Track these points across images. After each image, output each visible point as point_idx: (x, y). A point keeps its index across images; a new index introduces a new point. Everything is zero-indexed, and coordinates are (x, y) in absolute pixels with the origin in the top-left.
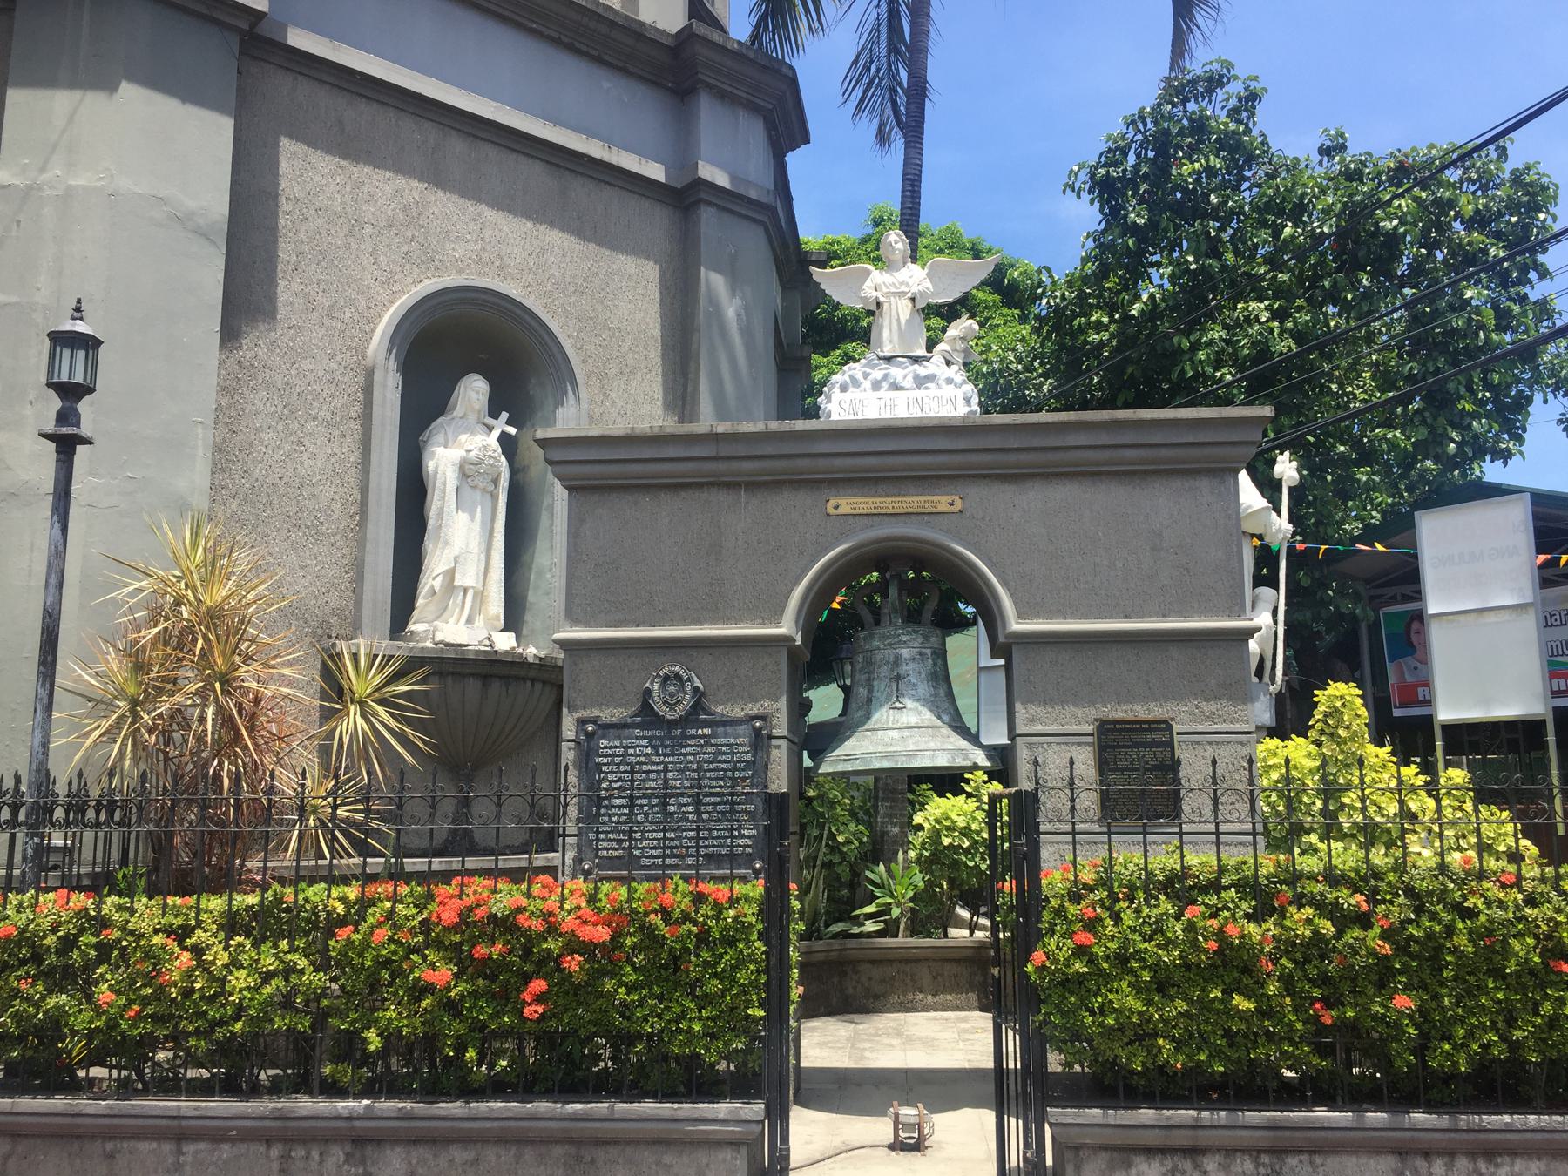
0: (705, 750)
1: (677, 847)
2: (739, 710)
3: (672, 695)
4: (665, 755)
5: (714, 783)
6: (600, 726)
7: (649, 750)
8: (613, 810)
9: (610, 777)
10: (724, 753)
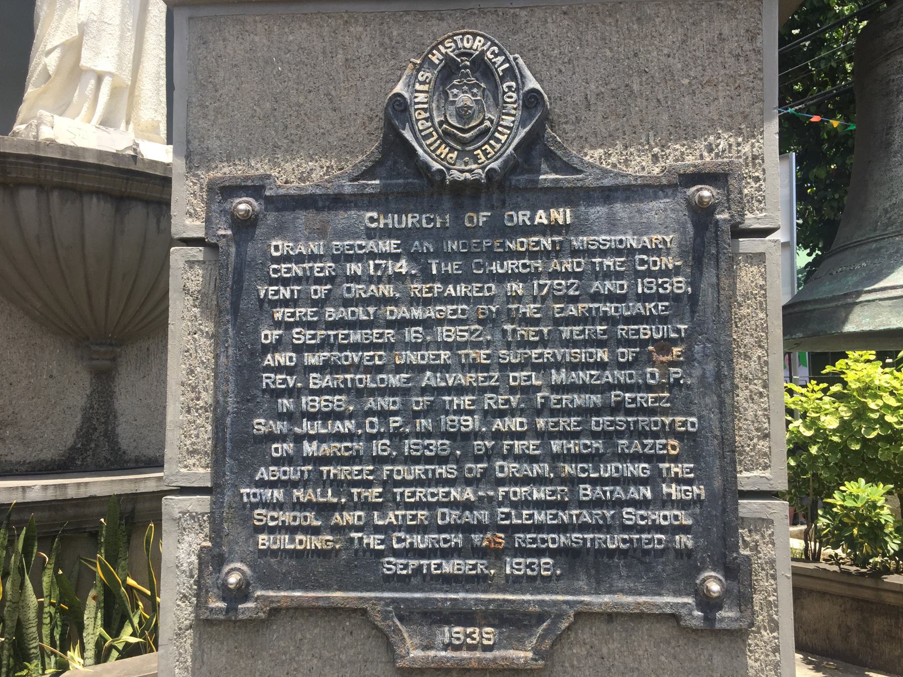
0: (554, 265)
1: (481, 528)
2: (646, 161)
3: (463, 114)
4: (446, 279)
5: (581, 354)
6: (270, 201)
7: (403, 266)
8: (306, 426)
9: (301, 336)
10: (608, 275)
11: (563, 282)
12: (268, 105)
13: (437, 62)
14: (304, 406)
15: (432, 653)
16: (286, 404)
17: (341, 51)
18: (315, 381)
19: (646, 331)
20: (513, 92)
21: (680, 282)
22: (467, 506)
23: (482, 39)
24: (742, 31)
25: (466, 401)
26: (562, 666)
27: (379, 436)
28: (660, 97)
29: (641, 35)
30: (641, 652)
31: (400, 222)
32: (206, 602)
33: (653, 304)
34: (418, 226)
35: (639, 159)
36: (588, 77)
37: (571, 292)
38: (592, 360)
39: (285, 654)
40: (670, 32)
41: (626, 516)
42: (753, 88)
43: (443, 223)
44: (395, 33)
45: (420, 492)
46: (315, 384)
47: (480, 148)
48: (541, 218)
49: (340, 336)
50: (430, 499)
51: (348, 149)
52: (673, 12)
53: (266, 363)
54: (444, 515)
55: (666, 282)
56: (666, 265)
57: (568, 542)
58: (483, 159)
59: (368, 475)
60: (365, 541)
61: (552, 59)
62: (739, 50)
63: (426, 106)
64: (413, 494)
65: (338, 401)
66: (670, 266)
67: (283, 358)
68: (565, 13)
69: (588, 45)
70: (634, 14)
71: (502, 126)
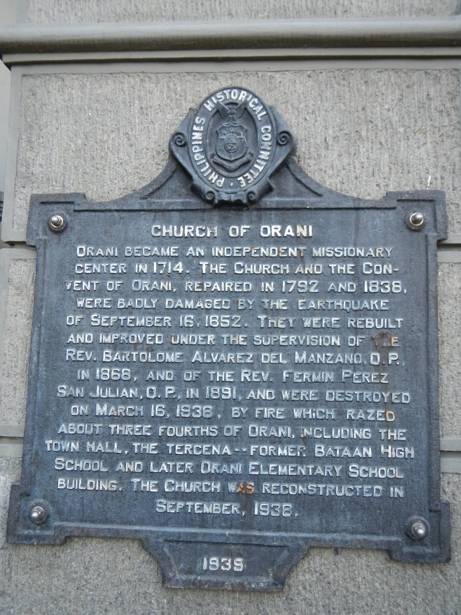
11: (306, 282)
12: (80, 141)
13: (210, 109)
14: (98, 376)
15: (193, 577)
16: (84, 374)
17: (137, 102)
18: (107, 356)
19: (370, 323)
20: (269, 133)
21: (398, 284)
22: (226, 459)
23: (245, 93)
24: (445, 93)
25: (227, 375)
26: (297, 589)
27: (157, 400)
28: (383, 140)
29: (368, 94)
30: (360, 580)
31: (178, 231)
32: (15, 529)
33: (376, 301)
34: (192, 235)
35: (366, 188)
36: (327, 124)
37: (312, 290)
38: (327, 345)
39: (76, 573)
40: (390, 92)
41: (351, 470)
42: (453, 136)
43: (212, 233)
44: (179, 89)
45: (188, 447)
46: (108, 358)
47: (242, 175)
48: (289, 231)
49: (129, 321)
50: (195, 453)
51: (140, 176)
52: (392, 78)
53: (70, 340)
54: (206, 465)
55: (387, 284)
56: (387, 271)
57: (304, 490)
58: (244, 185)
59: (146, 431)
60: (143, 485)
61: (300, 110)
62: (442, 108)
63: (201, 143)
64: (183, 448)
65: (126, 373)
66: (390, 272)
67: (83, 338)
68: (309, 76)
69: (327, 100)
70: (362, 78)
71: (259, 159)
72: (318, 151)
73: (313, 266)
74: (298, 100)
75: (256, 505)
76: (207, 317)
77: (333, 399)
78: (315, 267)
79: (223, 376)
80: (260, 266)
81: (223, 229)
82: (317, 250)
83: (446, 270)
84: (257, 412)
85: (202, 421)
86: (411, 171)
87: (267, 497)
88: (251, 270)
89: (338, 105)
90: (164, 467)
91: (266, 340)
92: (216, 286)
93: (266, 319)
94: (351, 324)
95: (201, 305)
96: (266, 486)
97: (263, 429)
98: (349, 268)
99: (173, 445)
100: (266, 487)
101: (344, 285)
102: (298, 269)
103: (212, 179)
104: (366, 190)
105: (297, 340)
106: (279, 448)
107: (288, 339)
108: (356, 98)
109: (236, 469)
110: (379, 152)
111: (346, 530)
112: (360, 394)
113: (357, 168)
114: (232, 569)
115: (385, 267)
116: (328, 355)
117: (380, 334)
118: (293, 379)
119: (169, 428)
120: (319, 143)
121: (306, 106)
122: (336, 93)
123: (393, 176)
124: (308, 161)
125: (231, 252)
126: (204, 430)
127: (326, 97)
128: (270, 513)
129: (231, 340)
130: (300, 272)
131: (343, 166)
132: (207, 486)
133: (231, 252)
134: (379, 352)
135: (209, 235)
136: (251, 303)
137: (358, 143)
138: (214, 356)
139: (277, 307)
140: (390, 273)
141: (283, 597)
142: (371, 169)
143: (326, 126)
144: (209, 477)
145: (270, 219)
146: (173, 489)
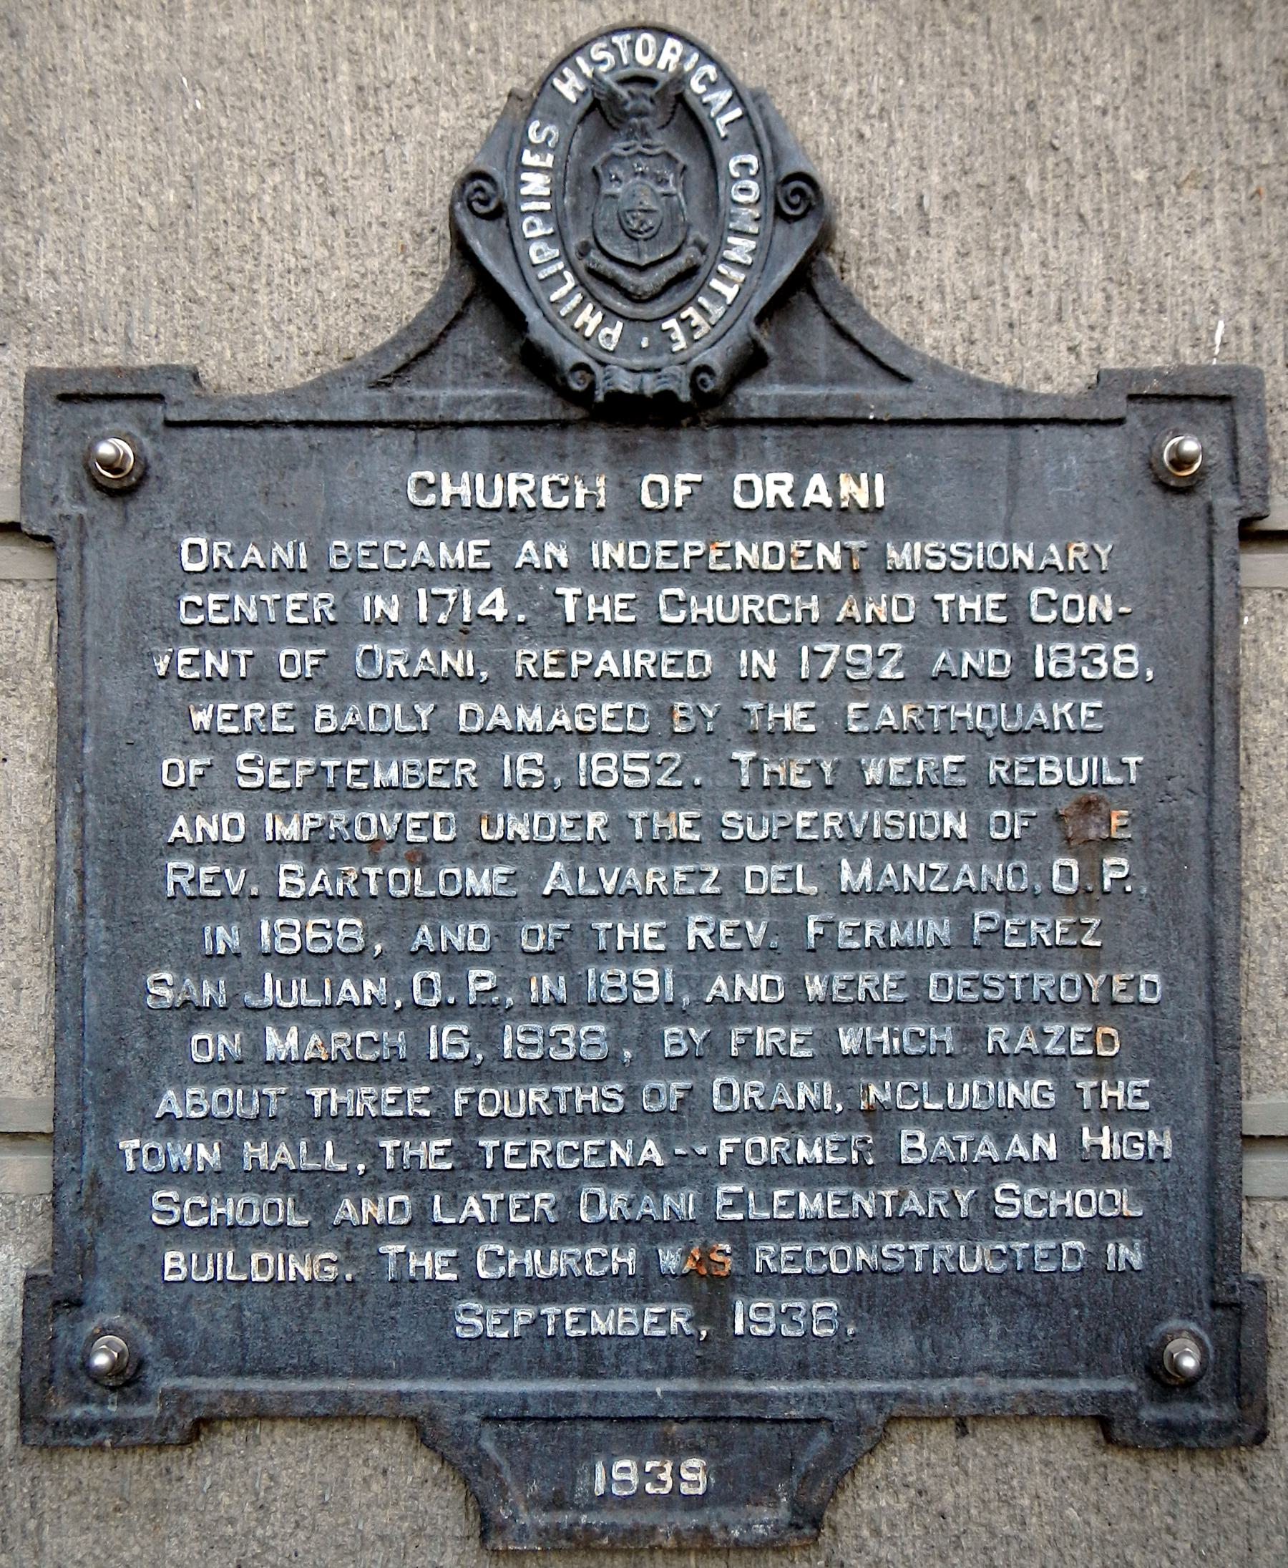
19: (1052, 770)
21: (1129, 652)
22: (650, 1178)
25: (647, 933)
28: (1087, 209)
33: (1069, 705)
37: (886, 673)
38: (931, 836)
45: (540, 1146)
47: (674, 313)
48: (817, 491)
55: (1099, 652)
56: (1098, 613)
61: (843, 106)
72: (899, 238)
73: (889, 600)
74: (838, 72)
75: (739, 1306)
76: (583, 757)
77: (949, 997)
78: (894, 602)
79: (636, 936)
80: (735, 599)
81: (622, 485)
82: (899, 551)
83: (1263, 611)
84: (735, 1039)
85: (579, 1068)
86: (1168, 305)
87: (770, 1283)
88: (708, 611)
89: (957, 91)
90: (473, 1208)
91: (758, 826)
92: (607, 662)
93: (754, 761)
94: (998, 775)
95: (565, 721)
96: (766, 1252)
97: (753, 1088)
98: (990, 606)
99: (497, 1143)
100: (765, 1254)
101: (977, 658)
102: (845, 608)
103: (585, 325)
104: (1039, 365)
105: (845, 823)
106: (800, 1143)
107: (818, 820)
108: (1010, 72)
109: (680, 1207)
110: (1076, 243)
111: (986, 1369)
112: (1025, 979)
113: (1012, 293)
114: (675, 1490)
115: (1094, 600)
116: (933, 866)
117: (1079, 803)
118: (835, 940)
119: (484, 1091)
120: (901, 212)
121: (861, 92)
122: (949, 51)
123: (1116, 320)
124: (871, 270)
125: (648, 558)
126: (586, 1097)
127: (921, 65)
128: (778, 1327)
129: (656, 826)
130: (853, 619)
131: (972, 288)
132: (598, 1258)
133: (648, 558)
134: (1076, 855)
135: (580, 503)
136: (710, 714)
137: (1016, 215)
138: (608, 878)
139: (788, 726)
140: (1108, 619)
141: (818, 1559)
142: (1053, 298)
143: (921, 159)
144: (604, 1231)
145: (762, 452)
146: (502, 1270)
